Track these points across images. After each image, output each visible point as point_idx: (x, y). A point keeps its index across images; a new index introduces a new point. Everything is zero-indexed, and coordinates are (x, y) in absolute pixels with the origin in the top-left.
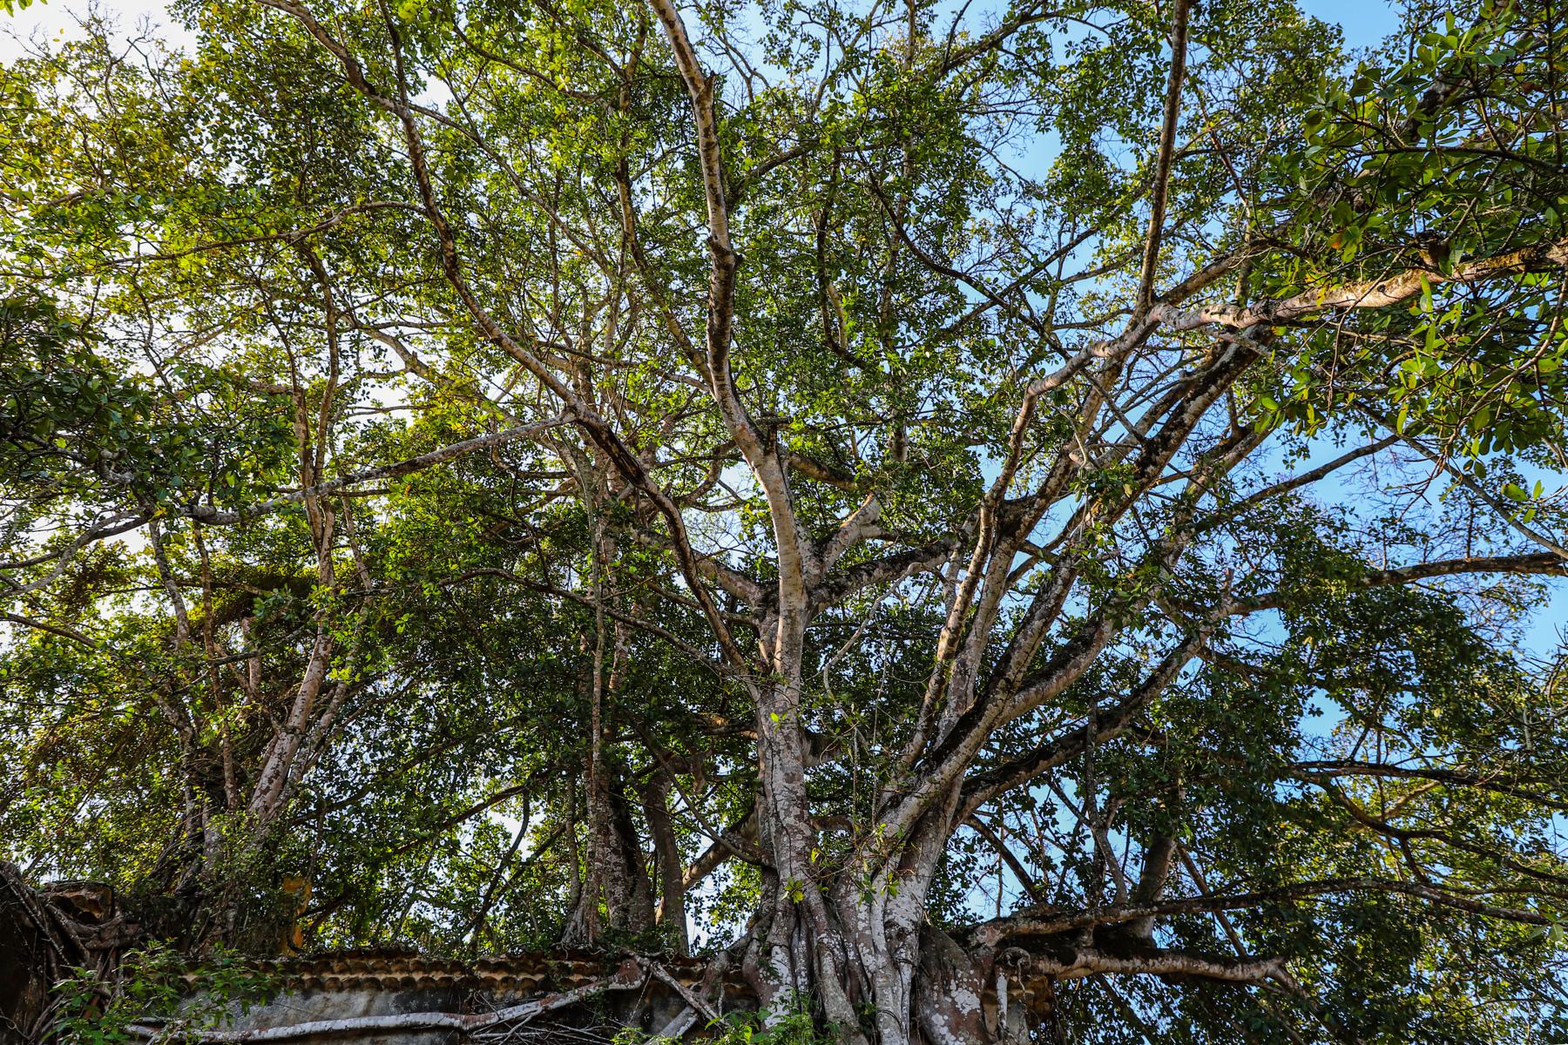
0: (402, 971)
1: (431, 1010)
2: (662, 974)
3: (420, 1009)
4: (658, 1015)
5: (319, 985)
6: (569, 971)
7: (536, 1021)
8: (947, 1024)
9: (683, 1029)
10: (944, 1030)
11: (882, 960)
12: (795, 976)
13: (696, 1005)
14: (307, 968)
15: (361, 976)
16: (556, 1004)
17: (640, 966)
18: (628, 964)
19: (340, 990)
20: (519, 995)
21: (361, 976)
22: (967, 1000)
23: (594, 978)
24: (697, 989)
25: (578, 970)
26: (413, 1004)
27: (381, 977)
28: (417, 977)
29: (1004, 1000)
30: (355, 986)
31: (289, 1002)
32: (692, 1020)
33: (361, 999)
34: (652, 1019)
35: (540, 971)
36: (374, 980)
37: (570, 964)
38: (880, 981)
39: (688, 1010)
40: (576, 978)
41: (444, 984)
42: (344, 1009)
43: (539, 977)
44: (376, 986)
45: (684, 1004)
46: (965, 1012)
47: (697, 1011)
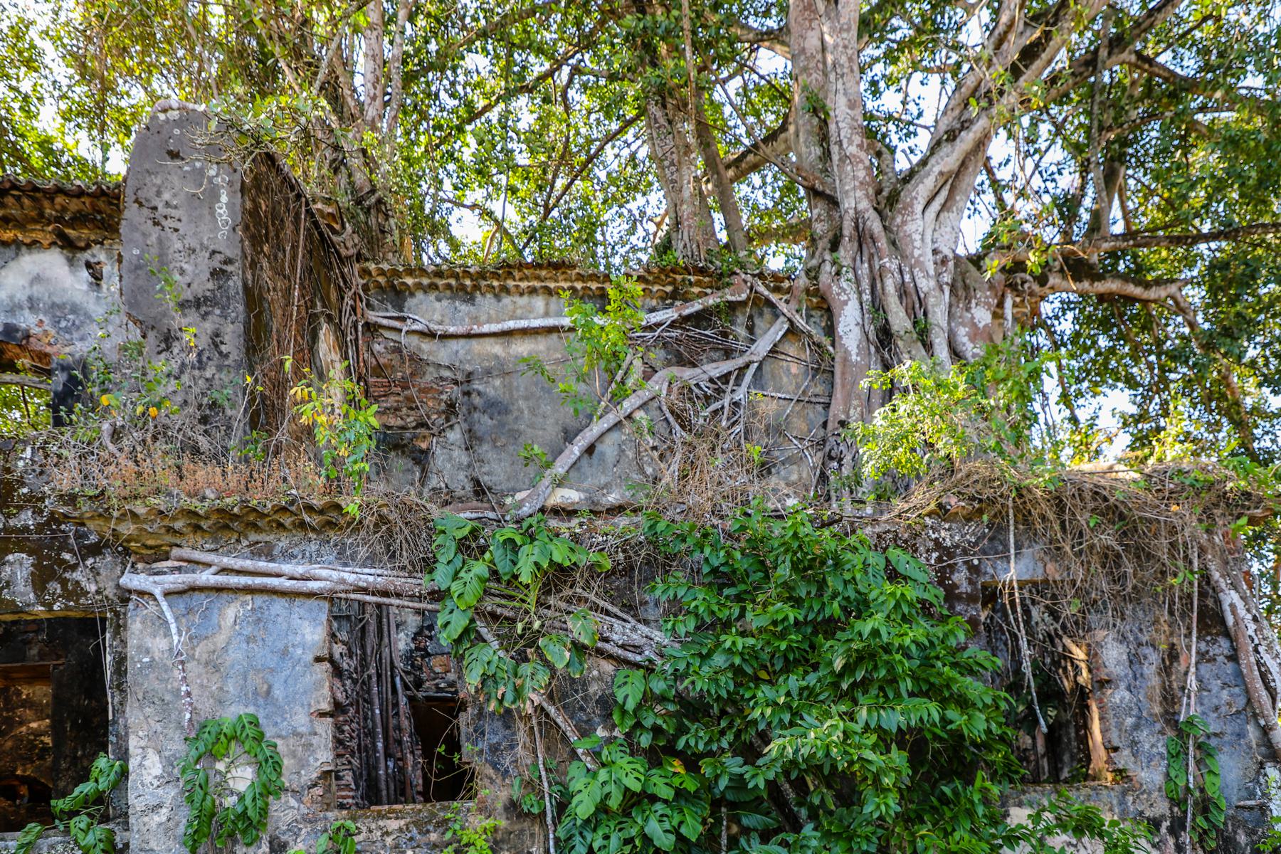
0: (565, 280)
2: (761, 289)
4: (757, 321)
5: (505, 290)
6: (691, 284)
7: (673, 325)
8: (967, 334)
9: (781, 333)
10: (965, 340)
11: (932, 283)
12: (860, 294)
13: (789, 315)
14: (496, 276)
15: (537, 284)
16: (686, 312)
17: (745, 282)
18: (735, 280)
19: (522, 294)
20: (654, 302)
21: (537, 284)
22: (982, 316)
23: (709, 291)
24: (787, 302)
25: (698, 283)
27: (552, 285)
28: (579, 285)
29: (1010, 317)
30: (533, 291)
31: (486, 303)
32: (786, 326)
33: (539, 302)
34: (753, 325)
35: (670, 284)
36: (546, 288)
37: (692, 279)
38: (931, 301)
39: (782, 319)
40: (696, 290)
41: (597, 293)
42: (529, 312)
43: (669, 289)
45: (776, 314)
46: (981, 325)
47: (789, 320)
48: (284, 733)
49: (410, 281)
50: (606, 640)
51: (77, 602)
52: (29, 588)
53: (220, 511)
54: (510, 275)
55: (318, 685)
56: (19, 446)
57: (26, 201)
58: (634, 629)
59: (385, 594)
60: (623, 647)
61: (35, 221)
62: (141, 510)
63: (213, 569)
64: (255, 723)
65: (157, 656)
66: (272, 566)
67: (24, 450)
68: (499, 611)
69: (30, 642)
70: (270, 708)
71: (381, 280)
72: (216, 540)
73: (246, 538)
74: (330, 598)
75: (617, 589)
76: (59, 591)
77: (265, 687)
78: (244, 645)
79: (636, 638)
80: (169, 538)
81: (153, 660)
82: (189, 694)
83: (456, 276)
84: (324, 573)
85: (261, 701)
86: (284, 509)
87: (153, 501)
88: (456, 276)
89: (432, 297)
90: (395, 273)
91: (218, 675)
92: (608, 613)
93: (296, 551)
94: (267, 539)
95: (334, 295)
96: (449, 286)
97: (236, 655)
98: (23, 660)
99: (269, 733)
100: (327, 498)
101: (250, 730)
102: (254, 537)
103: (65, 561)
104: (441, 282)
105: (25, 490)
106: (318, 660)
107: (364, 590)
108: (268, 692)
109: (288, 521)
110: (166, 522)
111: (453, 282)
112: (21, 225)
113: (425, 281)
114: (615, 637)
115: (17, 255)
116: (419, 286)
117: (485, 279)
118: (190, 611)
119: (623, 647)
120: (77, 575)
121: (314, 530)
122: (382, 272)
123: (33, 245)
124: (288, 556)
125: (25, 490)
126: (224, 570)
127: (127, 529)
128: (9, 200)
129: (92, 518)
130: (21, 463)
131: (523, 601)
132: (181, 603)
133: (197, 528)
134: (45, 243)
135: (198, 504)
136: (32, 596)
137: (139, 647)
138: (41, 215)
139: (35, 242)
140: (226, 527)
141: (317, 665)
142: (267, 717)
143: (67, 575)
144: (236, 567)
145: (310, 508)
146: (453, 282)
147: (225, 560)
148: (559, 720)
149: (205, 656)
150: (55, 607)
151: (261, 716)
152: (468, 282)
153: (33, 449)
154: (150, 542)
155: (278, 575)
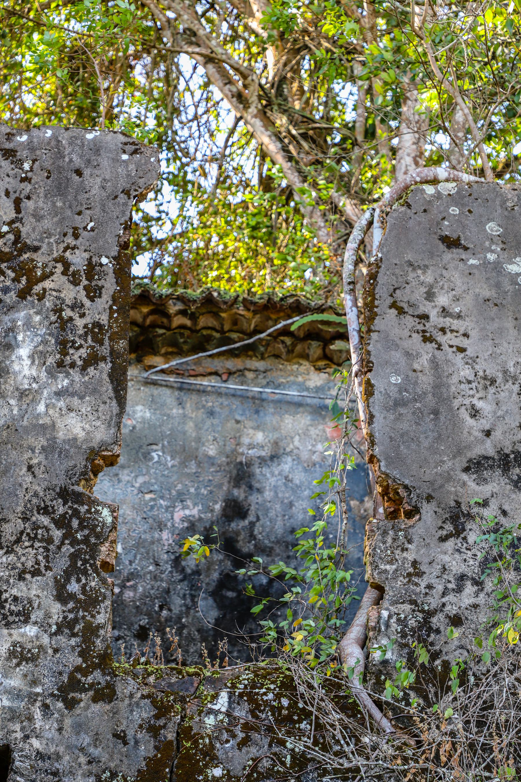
67: (215, 697)
105: (218, 772)
125: (218, 772)
130: (210, 721)
153: (231, 695)
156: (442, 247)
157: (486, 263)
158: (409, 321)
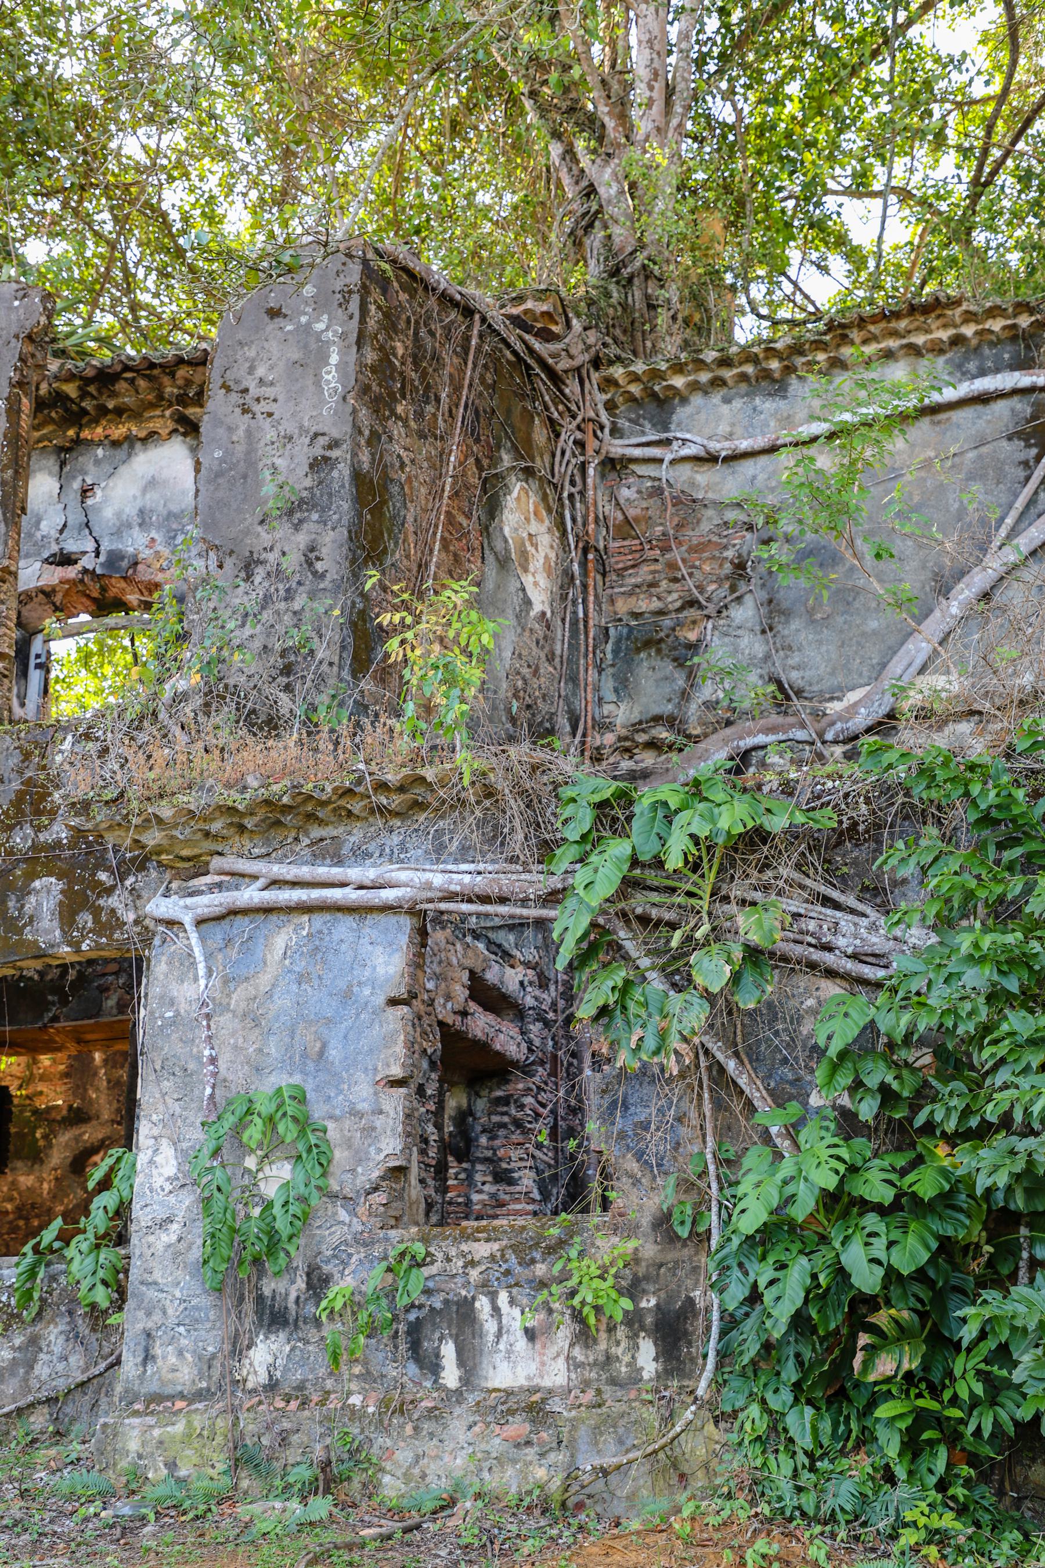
0: (945, 326)
1: (997, 370)
3: (982, 373)
14: (819, 345)
21: (893, 343)
26: (972, 366)
27: (920, 340)
28: (969, 330)
30: (889, 355)
33: (898, 372)
41: (1007, 334)
44: (914, 351)
48: (338, 1112)
49: (679, 382)
50: (828, 948)
51: (110, 937)
52: (56, 923)
53: (267, 802)
54: (844, 339)
55: (388, 1040)
56: (59, 736)
57: (142, 383)
58: (873, 928)
59: (485, 899)
60: (855, 957)
61: (152, 406)
62: (166, 811)
63: (261, 883)
64: (300, 1098)
65: (183, 1008)
66: (335, 872)
68: (654, 913)
69: (107, 989)
70: (323, 1076)
71: (635, 389)
72: (267, 842)
73: (307, 834)
74: (414, 911)
75: (855, 863)
76: (90, 924)
77: (318, 1045)
78: (294, 987)
79: (877, 942)
80: (208, 845)
81: (177, 1014)
82: (213, 1060)
83: (755, 360)
84: (403, 876)
85: (311, 1066)
86: (349, 792)
87: (182, 798)
88: (755, 360)
89: (716, 398)
90: (656, 374)
91: (257, 1031)
92: (837, 906)
93: (372, 847)
94: (335, 833)
95: (540, 435)
96: (744, 377)
97: (282, 1002)
98: (97, 1015)
99: (318, 1111)
100: (406, 771)
101: (291, 1108)
102: (316, 832)
103: (100, 883)
104: (728, 374)
106: (393, 1002)
107: (451, 897)
108: (321, 1053)
109: (357, 806)
110: (201, 825)
111: (749, 369)
112: (137, 415)
113: (704, 377)
114: (841, 942)
115: (129, 455)
116: (695, 386)
117: (802, 353)
118: (228, 942)
119: (855, 957)
120: (113, 901)
121: (397, 814)
122: (635, 378)
123: (150, 438)
124: (361, 855)
126: (275, 883)
127: (152, 838)
128: (122, 386)
129: (110, 828)
131: (690, 894)
132: (218, 933)
133: (242, 829)
134: (164, 432)
135: (238, 797)
136: (58, 933)
137: (162, 997)
138: (160, 397)
139: (152, 434)
140: (278, 823)
141: (391, 1010)
142: (317, 1089)
143: (101, 902)
144: (289, 877)
145: (382, 786)
146: (749, 369)
147: (276, 868)
148: (743, 1081)
149: (243, 1005)
150: (84, 947)
151: (309, 1087)
152: (775, 365)
154: (185, 853)
155: (343, 885)
156: (266, 319)
157: (299, 326)
158: (234, 397)
